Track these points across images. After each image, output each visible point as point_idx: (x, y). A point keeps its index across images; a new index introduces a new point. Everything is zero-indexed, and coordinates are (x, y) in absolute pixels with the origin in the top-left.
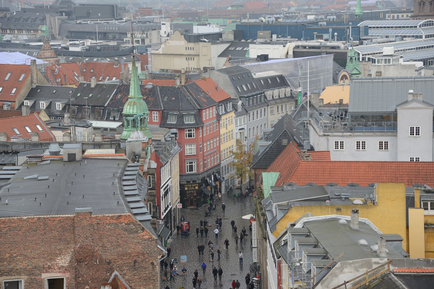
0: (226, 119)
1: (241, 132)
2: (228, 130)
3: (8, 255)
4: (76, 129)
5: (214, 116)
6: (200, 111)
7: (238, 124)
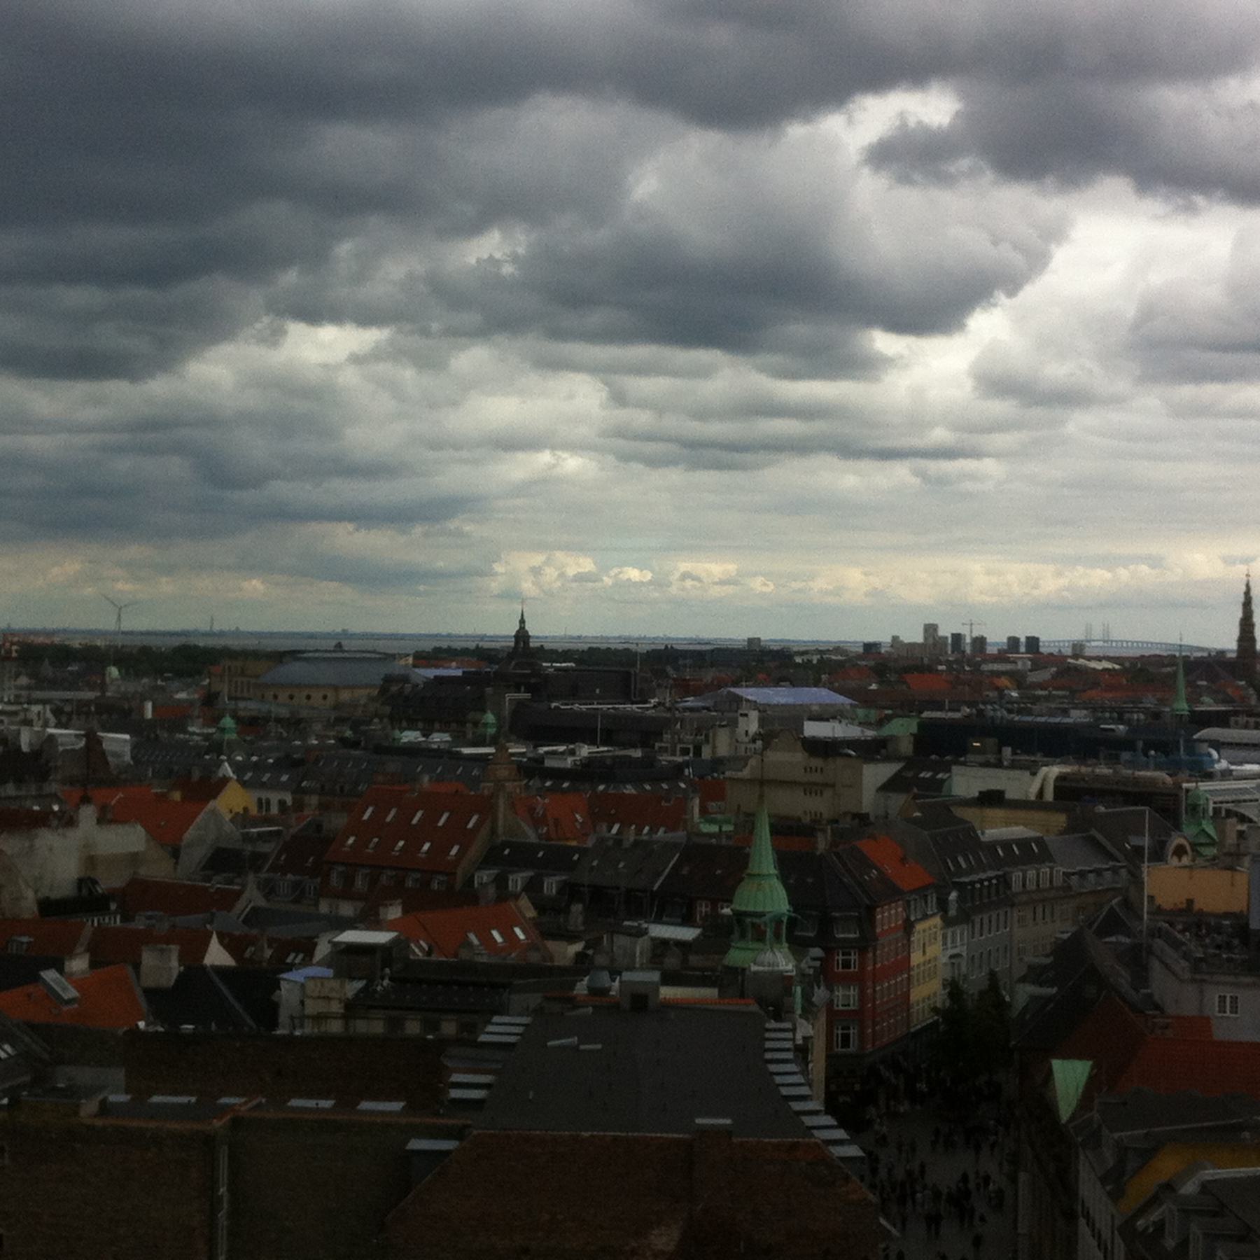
0: (924, 931)
1: (953, 964)
2: (927, 958)
4: (615, 939)
5: (900, 922)
6: (871, 910)
7: (949, 945)
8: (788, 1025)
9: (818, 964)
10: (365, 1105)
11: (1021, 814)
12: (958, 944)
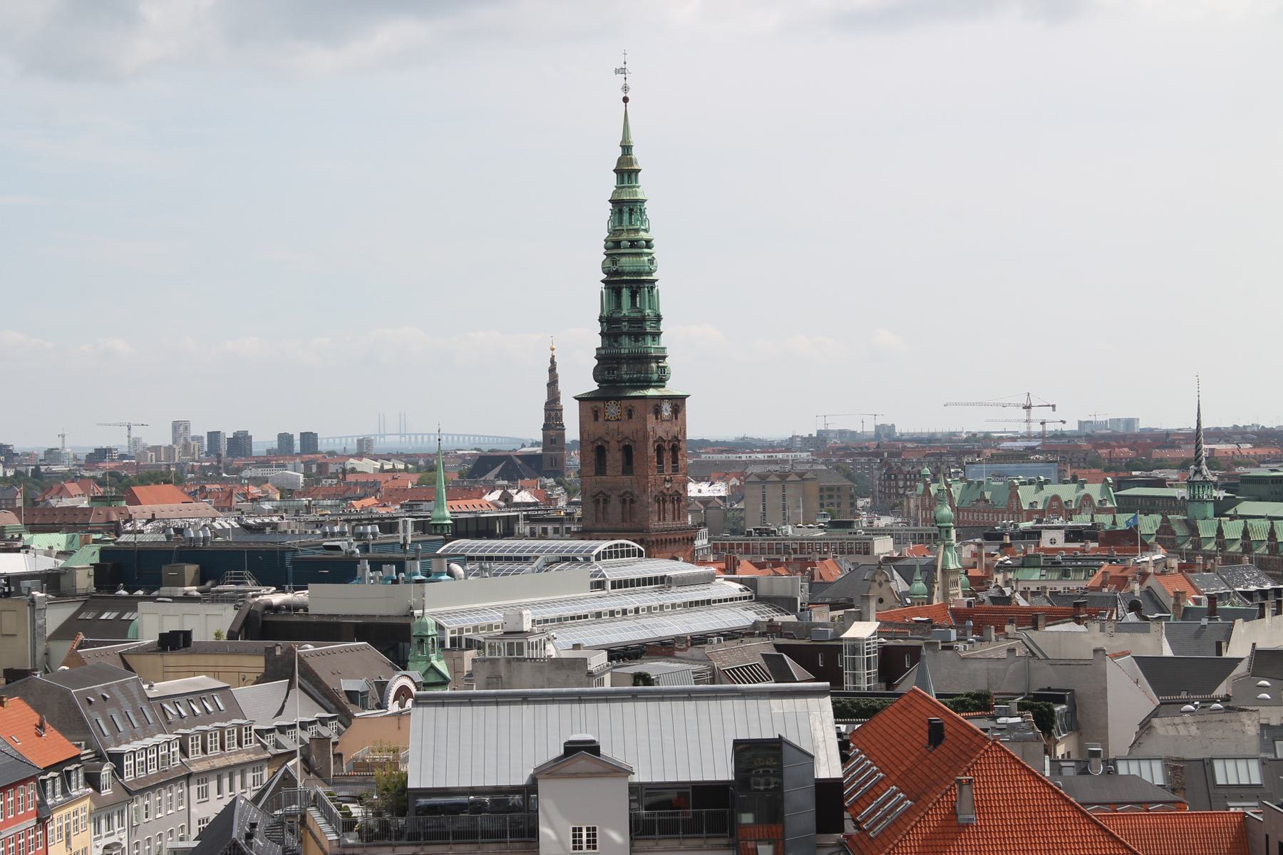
7: (104, 832)
11: (211, 660)
12: (117, 829)
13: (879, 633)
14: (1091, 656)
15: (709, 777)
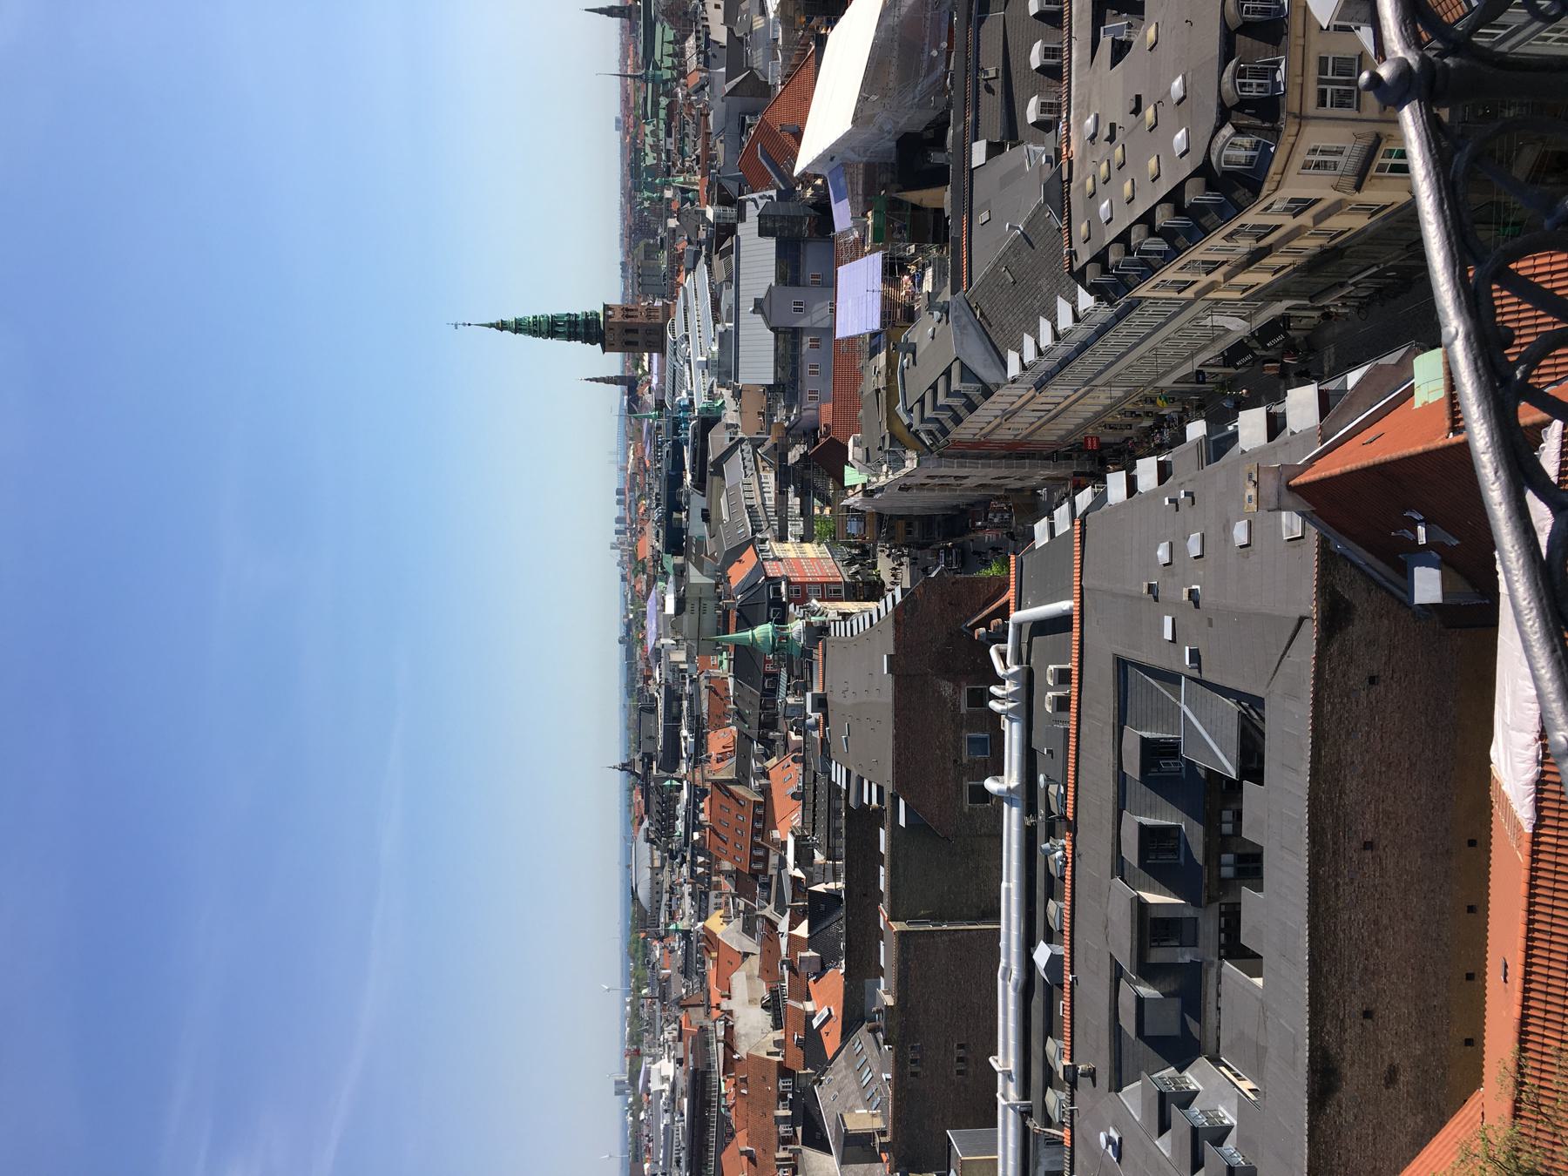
3: (938, 751)
8: (832, 624)
9: (797, 607)
10: (882, 850)
13: (712, 205)
14: (724, 104)
15: (775, 245)
